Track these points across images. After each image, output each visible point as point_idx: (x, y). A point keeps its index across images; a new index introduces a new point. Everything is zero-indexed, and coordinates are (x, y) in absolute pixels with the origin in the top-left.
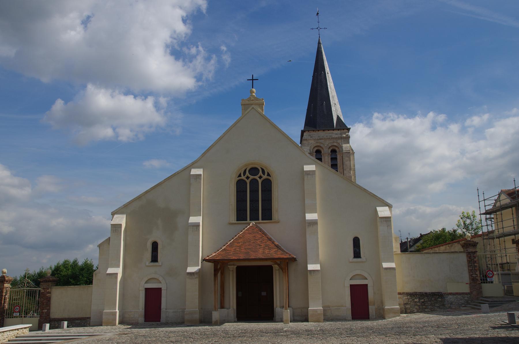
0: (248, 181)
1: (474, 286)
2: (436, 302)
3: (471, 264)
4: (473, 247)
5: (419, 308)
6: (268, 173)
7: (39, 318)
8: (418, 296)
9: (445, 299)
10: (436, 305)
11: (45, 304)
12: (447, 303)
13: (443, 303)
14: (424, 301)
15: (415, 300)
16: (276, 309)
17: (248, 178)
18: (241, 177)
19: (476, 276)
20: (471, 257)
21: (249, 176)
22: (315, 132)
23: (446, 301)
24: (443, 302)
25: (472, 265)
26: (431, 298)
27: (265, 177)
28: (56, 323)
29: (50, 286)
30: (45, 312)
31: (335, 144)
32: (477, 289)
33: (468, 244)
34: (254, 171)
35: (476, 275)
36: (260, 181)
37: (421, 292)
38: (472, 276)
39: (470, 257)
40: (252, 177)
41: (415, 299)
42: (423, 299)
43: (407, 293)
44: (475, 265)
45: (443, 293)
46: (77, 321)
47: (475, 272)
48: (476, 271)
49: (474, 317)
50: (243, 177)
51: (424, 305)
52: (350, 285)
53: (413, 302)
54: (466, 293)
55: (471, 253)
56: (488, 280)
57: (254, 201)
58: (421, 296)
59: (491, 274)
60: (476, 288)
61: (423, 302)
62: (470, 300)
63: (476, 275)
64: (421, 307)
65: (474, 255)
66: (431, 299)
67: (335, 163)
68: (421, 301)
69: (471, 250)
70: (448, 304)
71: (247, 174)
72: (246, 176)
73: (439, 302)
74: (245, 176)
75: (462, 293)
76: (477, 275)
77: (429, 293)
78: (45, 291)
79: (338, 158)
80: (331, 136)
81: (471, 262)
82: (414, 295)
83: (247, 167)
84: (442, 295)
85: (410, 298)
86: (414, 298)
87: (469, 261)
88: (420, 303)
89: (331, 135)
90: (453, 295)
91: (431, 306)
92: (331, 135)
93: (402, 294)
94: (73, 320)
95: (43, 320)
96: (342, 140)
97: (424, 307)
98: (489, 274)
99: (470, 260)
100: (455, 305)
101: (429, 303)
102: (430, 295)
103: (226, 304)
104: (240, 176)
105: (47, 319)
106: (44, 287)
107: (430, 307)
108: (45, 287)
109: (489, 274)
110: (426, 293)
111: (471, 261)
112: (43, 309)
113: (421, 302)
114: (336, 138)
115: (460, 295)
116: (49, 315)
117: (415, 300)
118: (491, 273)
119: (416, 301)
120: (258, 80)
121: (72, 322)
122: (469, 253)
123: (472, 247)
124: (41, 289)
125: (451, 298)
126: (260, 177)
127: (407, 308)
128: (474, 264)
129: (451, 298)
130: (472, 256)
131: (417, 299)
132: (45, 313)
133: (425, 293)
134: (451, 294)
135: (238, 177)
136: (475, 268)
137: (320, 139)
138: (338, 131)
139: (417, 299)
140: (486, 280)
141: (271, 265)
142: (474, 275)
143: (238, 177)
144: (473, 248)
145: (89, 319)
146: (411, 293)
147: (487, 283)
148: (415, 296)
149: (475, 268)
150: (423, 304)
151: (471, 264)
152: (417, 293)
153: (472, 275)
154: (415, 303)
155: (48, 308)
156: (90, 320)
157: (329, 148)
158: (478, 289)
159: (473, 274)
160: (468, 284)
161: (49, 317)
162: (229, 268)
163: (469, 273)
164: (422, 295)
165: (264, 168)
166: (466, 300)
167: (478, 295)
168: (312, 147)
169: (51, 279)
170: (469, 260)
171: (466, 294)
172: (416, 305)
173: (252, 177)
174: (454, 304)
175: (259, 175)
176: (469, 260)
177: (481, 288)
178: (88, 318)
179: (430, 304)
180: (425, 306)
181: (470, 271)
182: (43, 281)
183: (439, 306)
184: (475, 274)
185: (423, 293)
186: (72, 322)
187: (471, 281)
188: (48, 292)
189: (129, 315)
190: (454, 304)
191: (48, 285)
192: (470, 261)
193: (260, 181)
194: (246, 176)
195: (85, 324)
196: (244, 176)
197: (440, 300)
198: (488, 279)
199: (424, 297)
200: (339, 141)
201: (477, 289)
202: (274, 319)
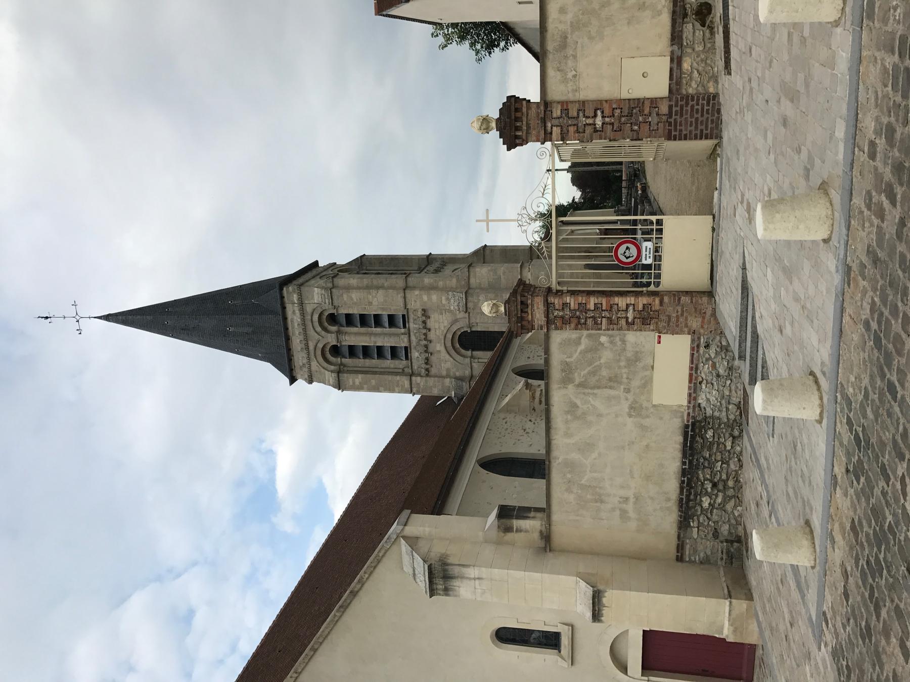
1: (669, 320)
2: (718, 445)
3: (590, 322)
4: (530, 307)
5: (733, 499)
8: (692, 497)
9: (710, 417)
10: (729, 448)
12: (724, 414)
13: (723, 426)
14: (711, 481)
15: (704, 506)
19: (634, 310)
20: (562, 317)
22: (293, 356)
23: (717, 414)
24: (720, 425)
25: (594, 318)
26: (702, 460)
31: (316, 317)
32: (682, 315)
33: (520, 325)
35: (631, 308)
37: (678, 485)
38: (633, 323)
39: (565, 322)
41: (702, 507)
42: (703, 484)
43: (680, 528)
44: (592, 308)
45: (688, 421)
47: (619, 311)
48: (616, 307)
49: (832, 595)
51: (725, 482)
53: (711, 512)
54: (692, 349)
55: (551, 316)
56: (649, 261)
58: (692, 487)
59: (627, 248)
60: (677, 316)
61: (715, 485)
62: (718, 338)
63: (631, 308)
64: (730, 492)
65: (557, 307)
66: (705, 459)
67: (358, 318)
68: (709, 490)
70: (727, 409)
75: (692, 362)
76: (628, 306)
77: (684, 463)
79: (346, 312)
80: (298, 324)
81: (583, 321)
82: (688, 508)
84: (693, 424)
86: (699, 508)
88: (717, 496)
89: (296, 325)
90: (695, 392)
91: (731, 461)
92: (296, 325)
93: (683, 542)
96: (306, 302)
97: (731, 483)
98: (627, 258)
99: (574, 321)
100: (733, 387)
102: (691, 462)
107: (732, 467)
109: (627, 258)
110: (684, 473)
111: (579, 318)
114: (303, 314)
115: (697, 369)
117: (706, 504)
118: (623, 247)
119: (710, 504)
122: (549, 322)
123: (530, 312)
125: (708, 400)
127: (730, 533)
128: (587, 311)
129: (708, 400)
130: (561, 314)
134: (692, 396)
136: (604, 308)
137: (307, 348)
138: (288, 309)
139: (704, 499)
140: (648, 267)
142: (630, 315)
144: (532, 305)
146: (681, 516)
147: (659, 267)
149: (604, 308)
150: (721, 487)
151: (590, 322)
152: (682, 499)
153: (630, 320)
154: (717, 509)
157: (325, 329)
158: (679, 309)
159: (627, 318)
160: (660, 337)
163: (620, 329)
164: (689, 484)
166: (717, 353)
167: (705, 313)
168: (325, 365)
170: (573, 325)
171: (695, 348)
172: (724, 506)
174: (730, 391)
176: (573, 325)
177: (677, 295)
179: (724, 465)
180: (728, 479)
181: (615, 327)
183: (731, 438)
184: (626, 310)
185: (683, 482)
187: (652, 328)
190: (730, 391)
192: (579, 323)
198: (644, 262)
199: (698, 478)
200: (309, 309)
201: (682, 315)
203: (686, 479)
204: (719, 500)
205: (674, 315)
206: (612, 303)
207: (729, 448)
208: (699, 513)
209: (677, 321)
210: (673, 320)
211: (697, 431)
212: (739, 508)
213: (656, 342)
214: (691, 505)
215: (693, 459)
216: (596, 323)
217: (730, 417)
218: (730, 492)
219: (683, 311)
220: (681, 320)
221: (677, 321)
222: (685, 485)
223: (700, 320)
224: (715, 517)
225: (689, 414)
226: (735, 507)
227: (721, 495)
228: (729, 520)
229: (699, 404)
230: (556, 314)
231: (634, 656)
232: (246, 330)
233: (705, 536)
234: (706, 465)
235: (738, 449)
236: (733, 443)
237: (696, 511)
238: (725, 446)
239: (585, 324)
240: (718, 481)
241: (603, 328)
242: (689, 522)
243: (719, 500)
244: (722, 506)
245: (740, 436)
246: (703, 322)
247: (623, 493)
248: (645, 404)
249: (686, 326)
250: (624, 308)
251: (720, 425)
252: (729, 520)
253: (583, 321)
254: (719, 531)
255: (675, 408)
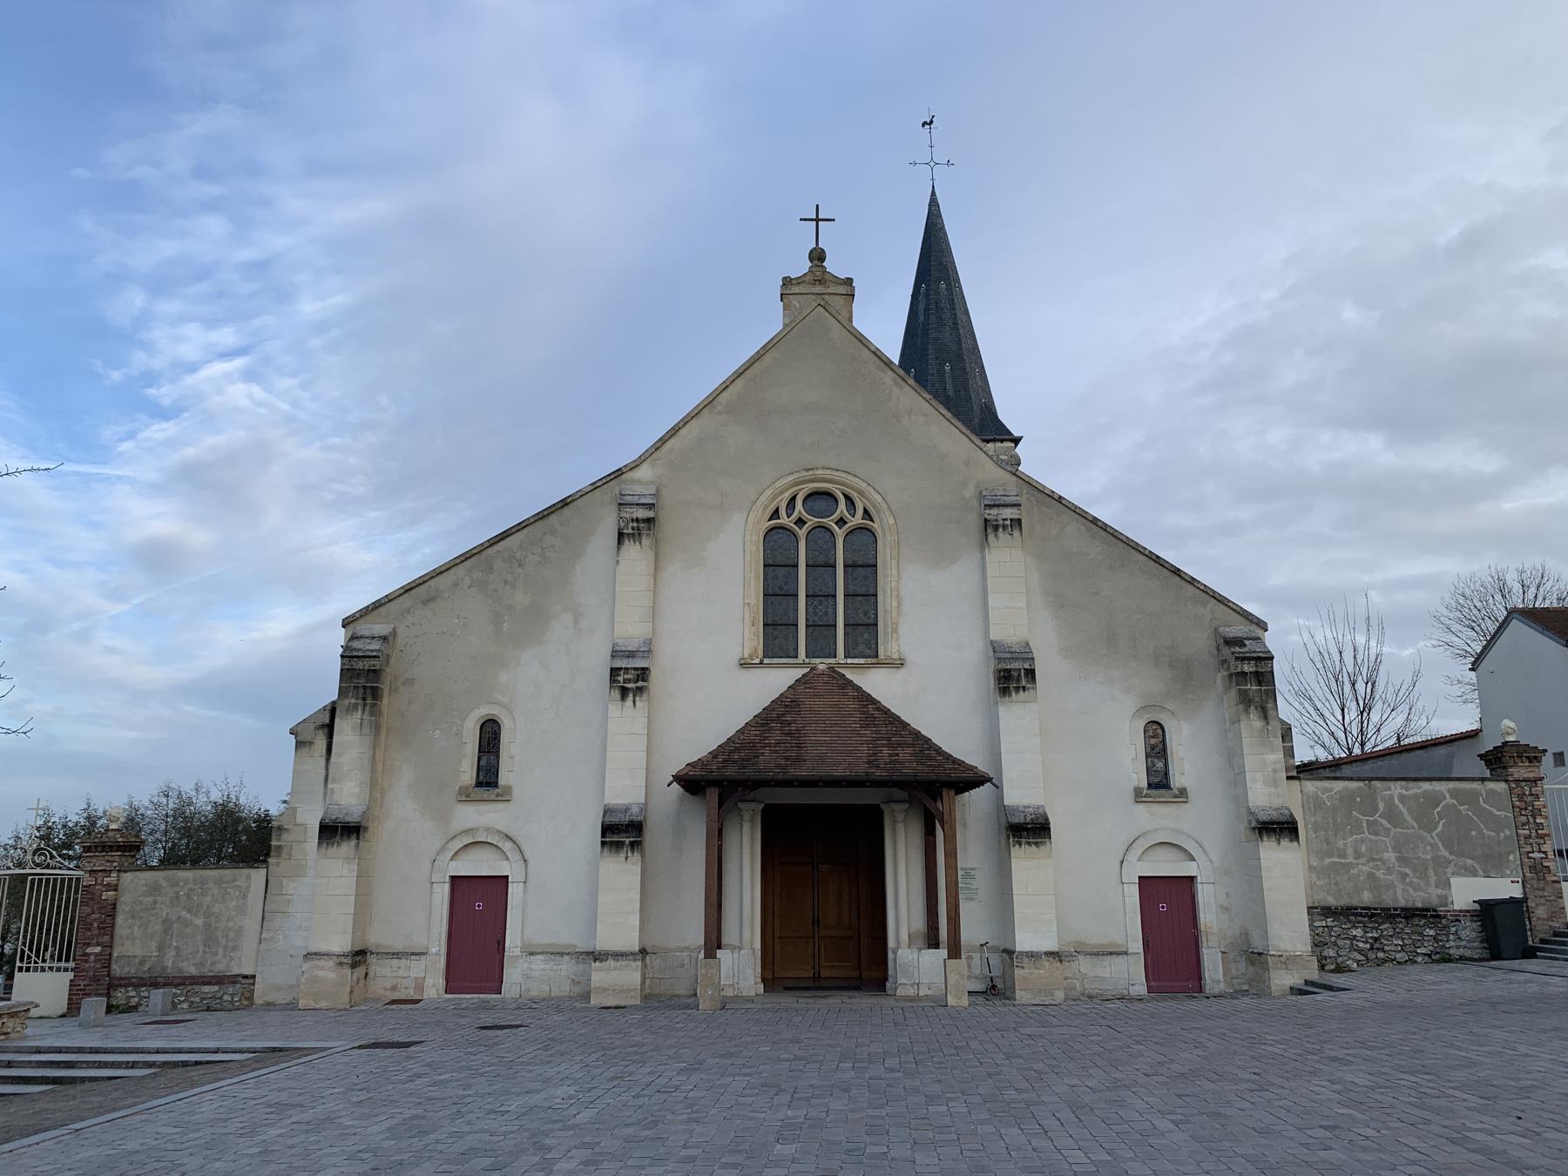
0: (802, 533)
2: (1420, 940)
3: (1524, 818)
5: (1363, 958)
6: (866, 511)
7: (71, 975)
11: (95, 925)
12: (1452, 944)
14: (1381, 935)
16: (895, 953)
17: (800, 522)
18: (779, 518)
19: (1541, 858)
20: (1524, 794)
21: (806, 516)
23: (1451, 937)
24: (1441, 941)
25: (1528, 822)
26: (1401, 926)
27: (857, 520)
28: (133, 994)
29: (115, 864)
30: (97, 955)
32: (1547, 901)
34: (821, 498)
35: (1543, 855)
36: (840, 533)
40: (812, 521)
42: (1377, 929)
43: (1323, 908)
44: (1538, 821)
45: (1441, 911)
46: (206, 989)
47: (1539, 845)
48: (1542, 841)
50: (784, 520)
52: (1139, 877)
55: (1524, 784)
57: (821, 597)
61: (1376, 939)
63: (1543, 855)
66: (1403, 929)
68: (1370, 935)
69: (1521, 771)
71: (800, 512)
72: (795, 516)
73: (1430, 941)
74: (790, 519)
76: (1545, 853)
77: (1395, 909)
78: (99, 882)
83: (797, 488)
85: (1335, 926)
86: (1349, 926)
87: (1518, 807)
88: (1366, 942)
94: (192, 984)
95: (86, 983)
97: (1381, 955)
99: (1523, 805)
101: (1395, 942)
102: (1399, 915)
103: (730, 934)
104: (775, 514)
105: (99, 980)
106: (95, 868)
107: (1398, 956)
108: (99, 868)
111: (1526, 809)
112: (89, 945)
113: (1372, 938)
116: (109, 967)
119: (1356, 936)
120: (834, 220)
121: (188, 991)
124: (83, 873)
126: (841, 522)
131: (1357, 928)
132: (93, 957)
133: (1381, 909)
135: (770, 519)
139: (1359, 930)
141: (878, 805)
143: (770, 519)
145: (252, 981)
148: (1352, 918)
153: (1530, 855)
154: (1352, 944)
155: (107, 938)
156: (254, 984)
158: (1552, 898)
159: (1533, 852)
160: (1518, 882)
161: (109, 971)
162: (742, 810)
164: (1373, 915)
165: (854, 495)
169: (120, 840)
172: (1355, 950)
173: (812, 521)
175: (836, 516)
178: (246, 977)
180: (1384, 951)
181: (1523, 842)
182: (90, 847)
185: (1375, 909)
186: (188, 991)
188: (108, 884)
189: (392, 967)
191: (108, 861)
193: (840, 533)
194: (795, 516)
195: (236, 999)
196: (788, 517)
197: (1432, 932)
199: (1382, 923)
201: (1547, 901)
202: (888, 985)
203: (1379, 911)
204: (1361, 945)
205: (1546, 894)
206: (1546, 838)
207: (1419, 951)
208: (1343, 926)
209: (1541, 897)
210: (1541, 893)
211: (1431, 920)
212: (1355, 964)
213: (1514, 879)
214: (1351, 918)
215: (1402, 918)
216: (1524, 824)
217: (1451, 950)
218: (1372, 955)
219: (1550, 901)
220: (1542, 900)
221: (1541, 897)
222: (1372, 911)
223: (1545, 916)
224: (1340, 942)
225: (1449, 911)
226: (1358, 962)
227: (1368, 946)
228: (1340, 956)
229: (1459, 921)
230: (1526, 788)
231: (1165, 866)
232: (949, 387)
233: (1318, 935)
234: (1397, 930)
235: (1420, 959)
236: (1425, 954)
237: (1345, 923)
238: (1419, 947)
239: (1521, 815)
240: (1381, 943)
241: (1520, 831)
242: (1331, 917)
243: (1361, 945)
244: (1355, 948)
245: (1434, 961)
246: (1544, 919)
247: (1350, 851)
248: (1449, 871)
249: (1537, 905)
250: (1543, 850)
251: (1441, 941)
252: (1340, 956)
253: (1523, 813)
254: (1326, 947)
255: (1450, 900)
